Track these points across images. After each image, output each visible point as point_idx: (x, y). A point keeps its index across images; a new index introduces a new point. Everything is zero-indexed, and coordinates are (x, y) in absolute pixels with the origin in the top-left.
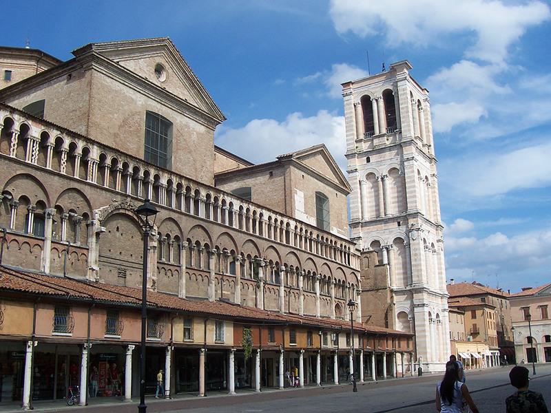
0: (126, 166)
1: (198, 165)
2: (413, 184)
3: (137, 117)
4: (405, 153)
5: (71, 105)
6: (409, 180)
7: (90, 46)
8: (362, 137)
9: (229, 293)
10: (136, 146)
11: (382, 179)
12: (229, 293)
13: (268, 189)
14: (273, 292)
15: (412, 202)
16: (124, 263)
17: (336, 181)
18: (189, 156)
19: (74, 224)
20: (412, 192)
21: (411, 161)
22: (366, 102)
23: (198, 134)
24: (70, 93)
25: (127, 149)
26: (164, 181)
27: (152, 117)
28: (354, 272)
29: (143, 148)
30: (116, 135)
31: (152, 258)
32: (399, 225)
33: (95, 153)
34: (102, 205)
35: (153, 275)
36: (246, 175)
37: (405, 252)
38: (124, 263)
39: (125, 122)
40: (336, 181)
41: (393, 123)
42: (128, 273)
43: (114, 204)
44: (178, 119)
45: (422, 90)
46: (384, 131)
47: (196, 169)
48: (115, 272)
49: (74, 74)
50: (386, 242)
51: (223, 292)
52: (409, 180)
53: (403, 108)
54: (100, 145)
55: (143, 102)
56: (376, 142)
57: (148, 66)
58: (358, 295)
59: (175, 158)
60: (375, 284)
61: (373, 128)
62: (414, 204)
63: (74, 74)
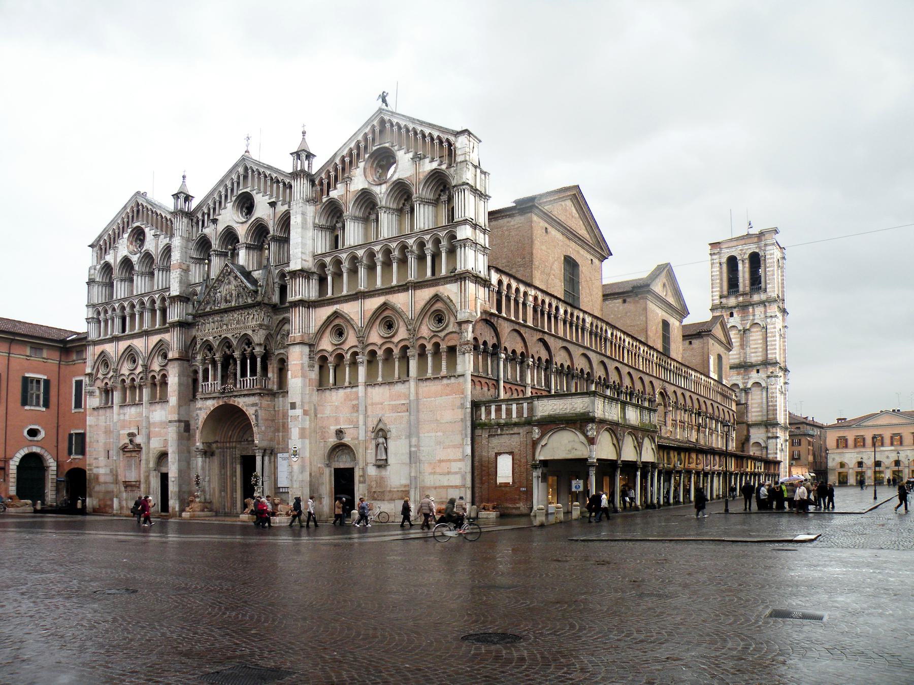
2: (774, 339)
4: (768, 311)
5: (628, 322)
6: (770, 335)
8: (725, 293)
11: (744, 332)
13: (688, 354)
15: (772, 354)
17: (723, 339)
20: (772, 345)
21: (774, 319)
22: (732, 262)
24: (626, 313)
32: (758, 371)
37: (762, 394)
40: (723, 339)
41: (756, 282)
45: (780, 248)
46: (748, 289)
49: (628, 300)
50: (745, 385)
52: (770, 335)
53: (769, 271)
56: (741, 299)
58: (734, 431)
61: (737, 286)
62: (774, 356)
63: (628, 300)
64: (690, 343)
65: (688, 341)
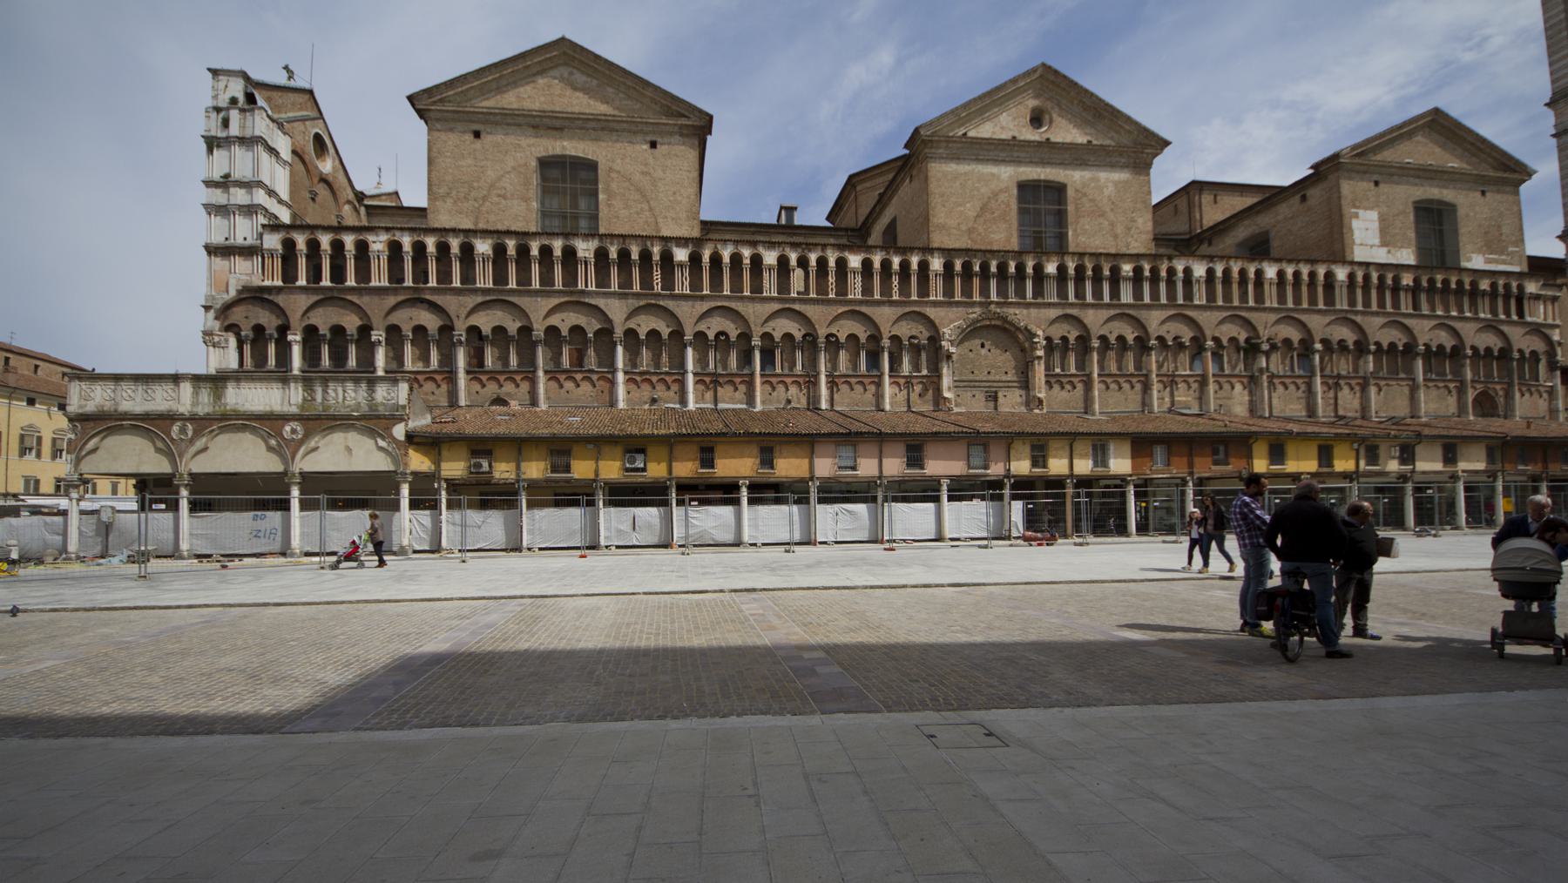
0: (985, 267)
1: (1119, 230)
3: (1002, 197)
7: (917, 131)
9: (1189, 399)
10: (1004, 235)
12: (1189, 399)
14: (1292, 387)
16: (995, 384)
18: (1101, 220)
19: (916, 350)
23: (1116, 184)
25: (991, 243)
26: (1051, 268)
27: (1026, 189)
29: (1015, 234)
30: (970, 231)
31: (1040, 370)
33: (936, 264)
34: (952, 321)
35: (1040, 392)
36: (1258, 212)
38: (995, 384)
39: (984, 208)
42: (1000, 394)
43: (971, 316)
44: (1074, 178)
47: (1116, 237)
48: (980, 396)
51: (1176, 399)
54: (942, 250)
55: (1007, 175)
57: (1015, 119)
59: (1075, 230)
63: (914, 173)
64: (1304, 198)
65: (1298, 197)
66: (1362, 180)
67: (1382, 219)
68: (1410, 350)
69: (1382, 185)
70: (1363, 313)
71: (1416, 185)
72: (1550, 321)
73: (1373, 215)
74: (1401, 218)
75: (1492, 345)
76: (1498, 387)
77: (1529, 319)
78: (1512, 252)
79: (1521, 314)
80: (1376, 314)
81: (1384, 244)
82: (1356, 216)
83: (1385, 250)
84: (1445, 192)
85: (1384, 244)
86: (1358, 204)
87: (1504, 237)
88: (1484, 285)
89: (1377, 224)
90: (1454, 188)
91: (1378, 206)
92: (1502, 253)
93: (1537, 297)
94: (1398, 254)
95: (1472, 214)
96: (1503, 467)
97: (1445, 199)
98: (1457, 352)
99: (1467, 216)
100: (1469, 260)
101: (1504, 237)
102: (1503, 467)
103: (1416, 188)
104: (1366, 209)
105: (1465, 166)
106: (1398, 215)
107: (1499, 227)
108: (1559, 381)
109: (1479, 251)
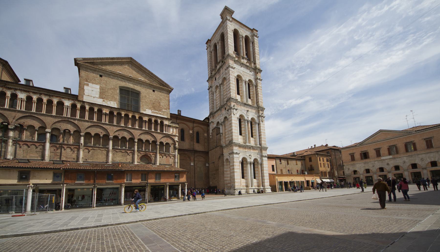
28: (168, 136)
60: (216, 145)
66: (93, 73)
67: (101, 89)
68: (106, 137)
69: (103, 77)
70: (78, 120)
71: (122, 81)
72: (174, 134)
73: (98, 87)
74: (112, 90)
75: (149, 139)
76: (151, 154)
77: (164, 132)
78: (164, 111)
79: (162, 130)
80: (87, 121)
81: (101, 97)
82: (88, 85)
83: (102, 100)
84: (136, 86)
85: (101, 97)
86: (89, 81)
87: (161, 106)
88: (146, 119)
89: (99, 90)
90: (141, 86)
91: (101, 84)
92: (160, 111)
93: (169, 126)
94: (109, 103)
95: (147, 96)
96: (94, 182)
97: (135, 89)
98: (132, 140)
99: (146, 96)
100: (145, 110)
101: (161, 106)
102: (94, 182)
103: (122, 82)
104: (93, 83)
105: (147, 81)
106: (111, 89)
107: (160, 102)
108: (177, 153)
109: (150, 109)
